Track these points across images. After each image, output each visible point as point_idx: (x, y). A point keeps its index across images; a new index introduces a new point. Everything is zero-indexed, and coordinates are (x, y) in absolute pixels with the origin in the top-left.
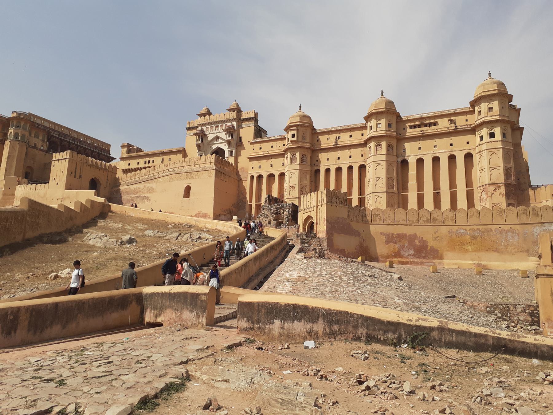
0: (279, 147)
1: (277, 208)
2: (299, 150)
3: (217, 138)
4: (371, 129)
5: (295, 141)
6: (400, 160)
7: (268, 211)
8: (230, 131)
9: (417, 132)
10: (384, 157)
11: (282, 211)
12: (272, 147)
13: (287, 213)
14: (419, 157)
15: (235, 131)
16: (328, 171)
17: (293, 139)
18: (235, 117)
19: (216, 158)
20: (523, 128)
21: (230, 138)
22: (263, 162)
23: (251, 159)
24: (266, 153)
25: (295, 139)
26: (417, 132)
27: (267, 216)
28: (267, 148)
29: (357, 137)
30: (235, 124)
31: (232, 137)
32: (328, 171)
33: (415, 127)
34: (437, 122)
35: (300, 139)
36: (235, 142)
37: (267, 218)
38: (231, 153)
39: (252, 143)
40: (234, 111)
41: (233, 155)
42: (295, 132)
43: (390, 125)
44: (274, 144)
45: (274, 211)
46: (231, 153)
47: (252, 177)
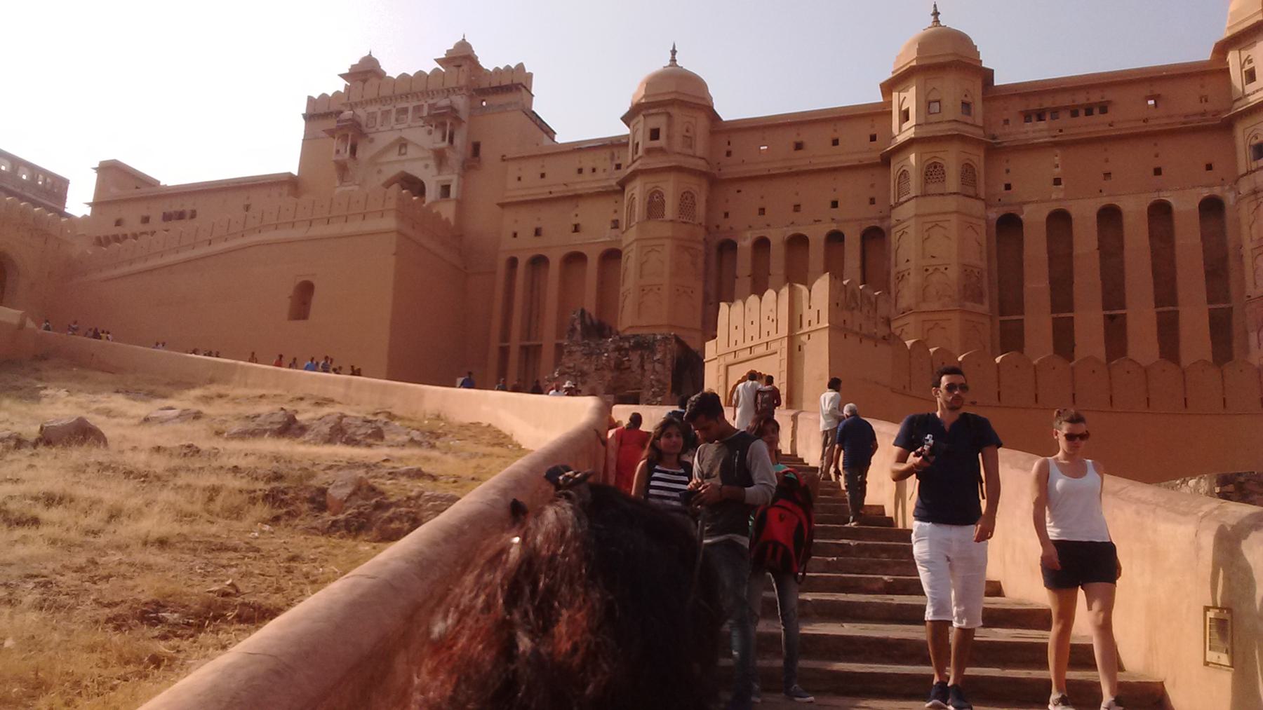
1: (619, 349)
3: (403, 144)
5: (661, 150)
6: (994, 215)
8: (444, 120)
12: (580, 171)
14: (1055, 206)
17: (656, 143)
24: (558, 191)
25: (661, 142)
31: (451, 141)
34: (1109, 102)
35: (678, 145)
38: (446, 190)
41: (453, 192)
44: (587, 162)
46: (446, 190)
47: (513, 262)
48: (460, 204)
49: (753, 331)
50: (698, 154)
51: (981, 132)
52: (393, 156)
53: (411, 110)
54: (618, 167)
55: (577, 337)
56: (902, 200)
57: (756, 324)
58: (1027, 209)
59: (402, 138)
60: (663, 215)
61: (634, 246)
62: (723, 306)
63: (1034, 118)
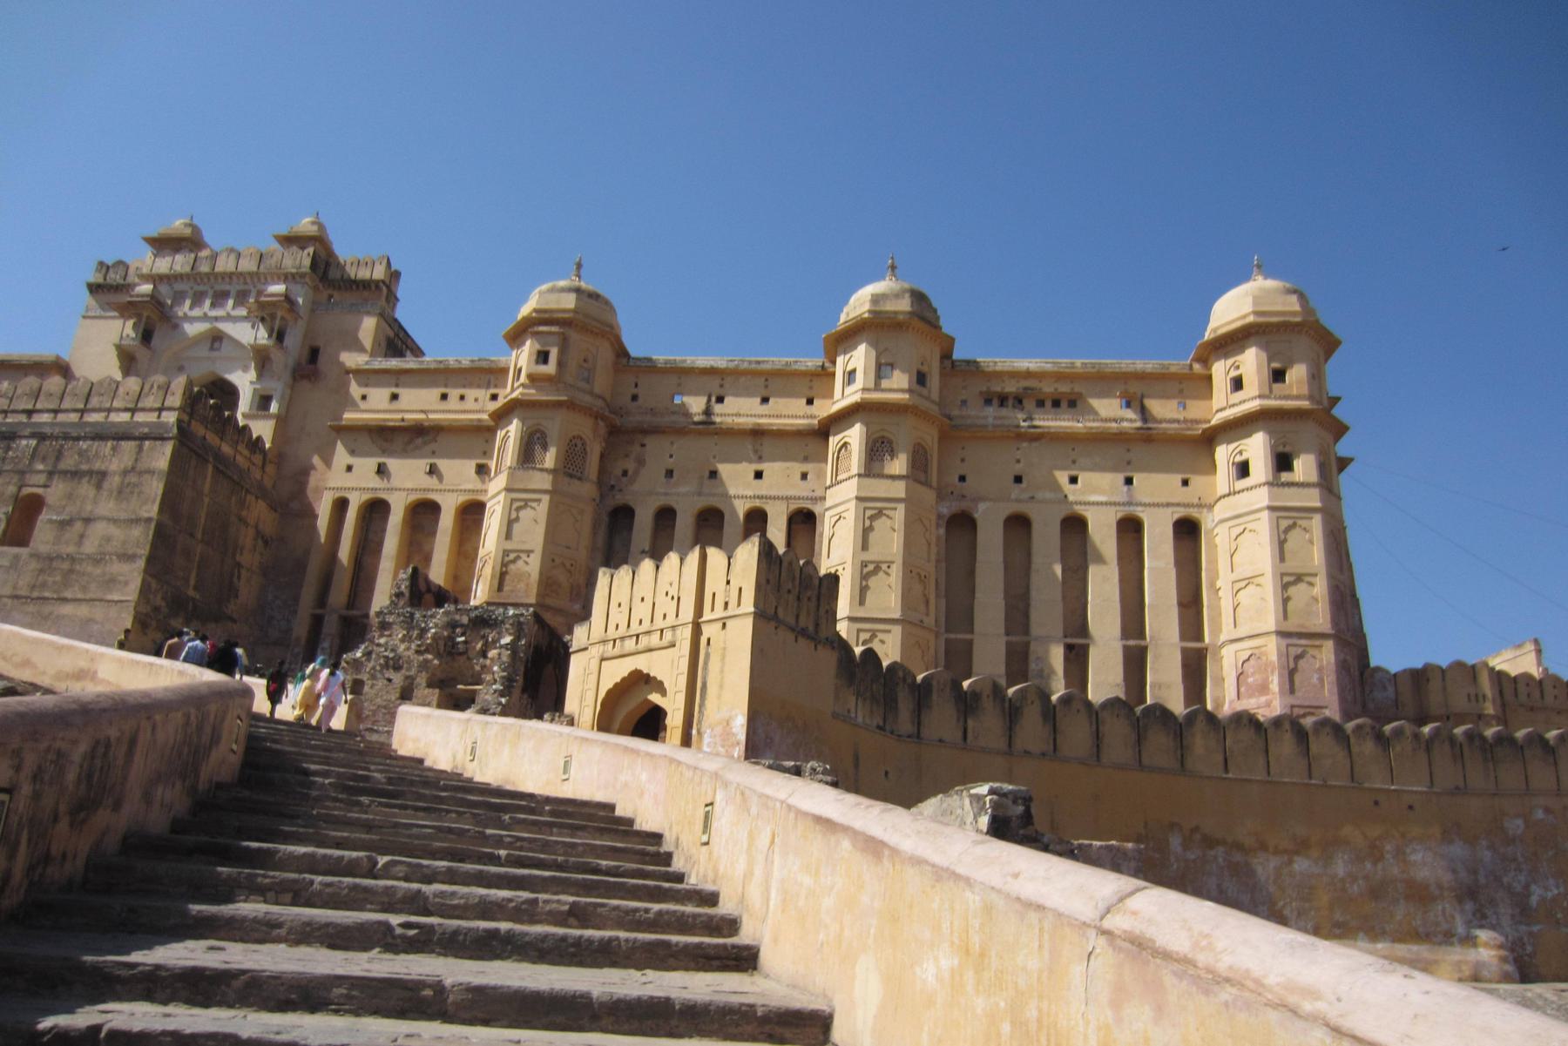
3: (217, 338)
5: (548, 379)
6: (946, 510)
10: (899, 489)
12: (444, 397)
15: (297, 317)
17: (543, 369)
25: (550, 368)
27: (395, 664)
36: (291, 362)
37: (397, 668)
38: (263, 401)
41: (274, 407)
43: (921, 379)
47: (341, 505)
48: (282, 421)
49: (642, 611)
50: (597, 390)
51: (936, 408)
52: (203, 351)
53: (233, 293)
57: (649, 602)
58: (982, 506)
61: (501, 497)
62: (603, 576)
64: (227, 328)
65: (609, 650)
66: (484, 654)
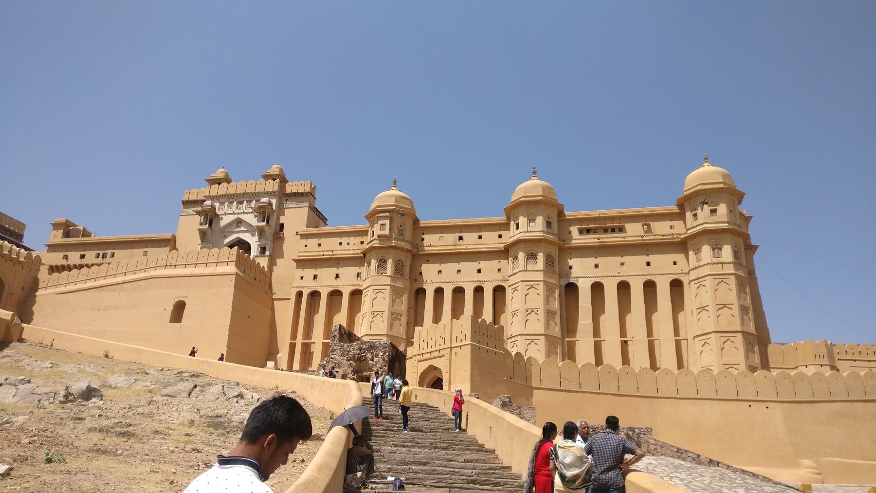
0: (352, 247)
1: (360, 349)
2: (392, 251)
3: (239, 222)
4: (518, 228)
5: (386, 236)
6: (564, 283)
7: (342, 355)
9: (590, 240)
10: (540, 276)
11: (369, 356)
12: (341, 244)
13: (381, 360)
16: (439, 292)
18: (276, 189)
19: (238, 255)
20: (756, 247)
21: (264, 224)
22: (321, 272)
23: (302, 263)
26: (590, 240)
28: (330, 247)
29: (491, 241)
30: (274, 201)
31: (268, 222)
32: (439, 292)
33: (588, 231)
36: (272, 231)
38: (263, 250)
39: (304, 236)
40: (274, 180)
41: (267, 253)
42: (387, 222)
43: (549, 224)
44: (344, 240)
45: (354, 355)
47: (300, 294)
54: (362, 243)
55: (337, 340)
56: (515, 271)
59: (239, 218)
60: (386, 272)
63: (585, 232)
64: (244, 217)
65: (420, 357)
66: (372, 359)
